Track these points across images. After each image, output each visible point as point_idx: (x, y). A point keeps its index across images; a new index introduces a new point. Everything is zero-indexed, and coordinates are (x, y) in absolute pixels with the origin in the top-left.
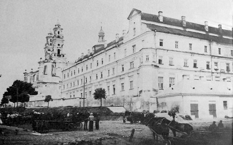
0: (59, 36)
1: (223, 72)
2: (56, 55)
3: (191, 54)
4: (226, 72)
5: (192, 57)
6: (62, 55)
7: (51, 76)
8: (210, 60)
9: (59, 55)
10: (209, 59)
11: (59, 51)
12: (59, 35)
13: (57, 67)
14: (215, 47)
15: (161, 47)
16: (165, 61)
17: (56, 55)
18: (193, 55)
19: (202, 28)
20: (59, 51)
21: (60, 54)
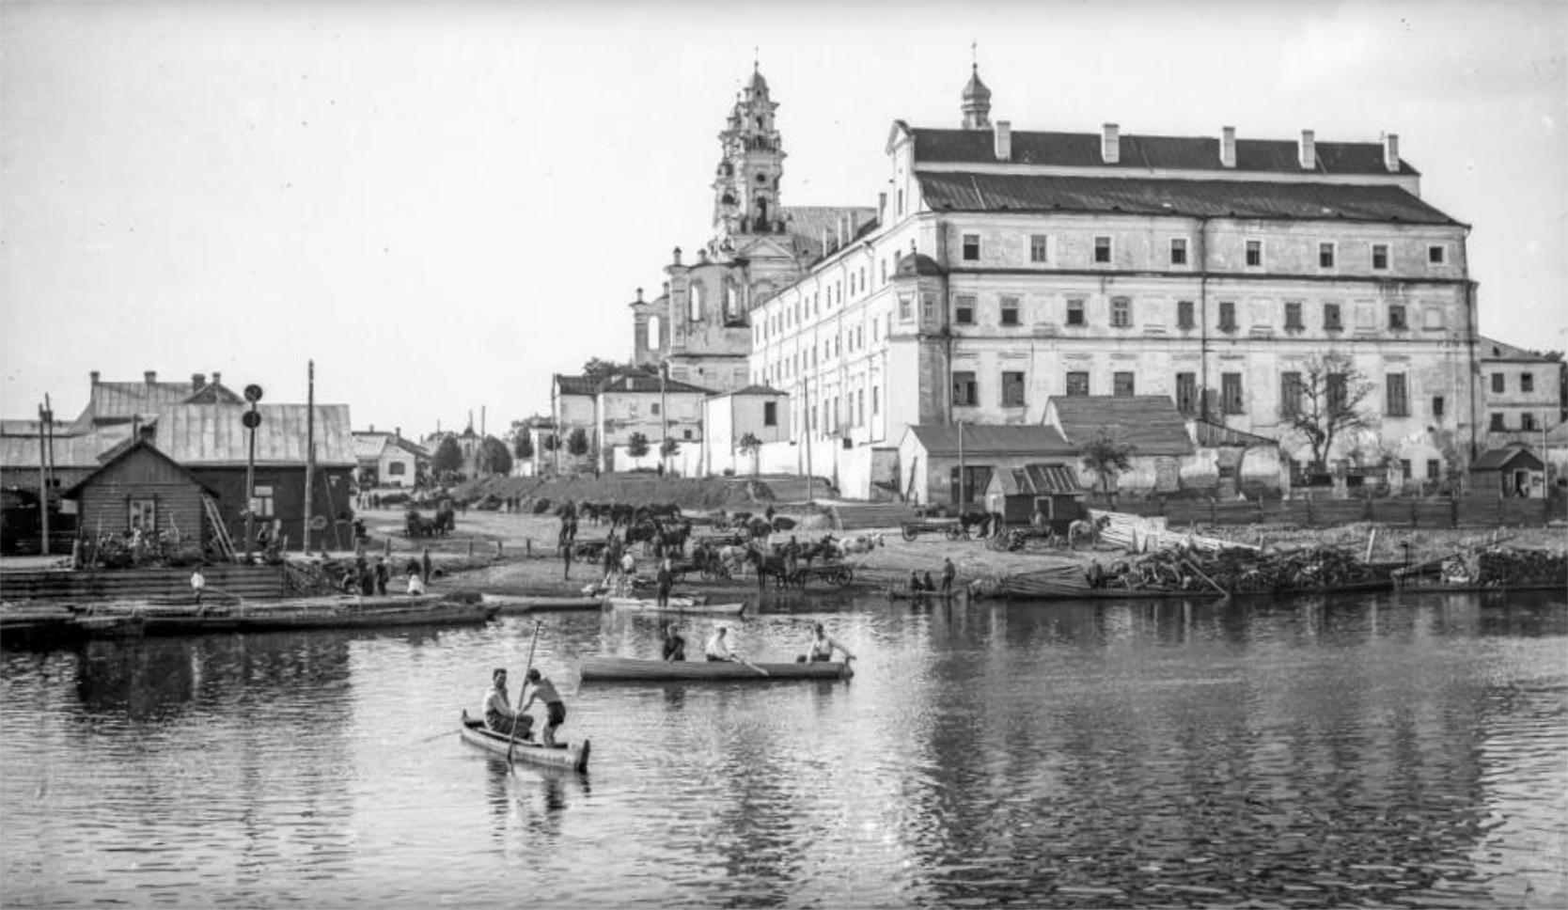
0: (759, 138)
1: (1264, 335)
2: (749, 225)
3: (1101, 278)
4: (1279, 331)
5: (1108, 286)
6: (775, 228)
7: (722, 324)
8: (1199, 294)
9: (762, 226)
10: (1190, 289)
11: (762, 203)
12: (762, 133)
13: (754, 277)
14: (1228, 239)
15: (969, 264)
16: (988, 313)
17: (749, 225)
18: (1108, 278)
19: (1203, 151)
20: (762, 203)
21: (769, 218)
